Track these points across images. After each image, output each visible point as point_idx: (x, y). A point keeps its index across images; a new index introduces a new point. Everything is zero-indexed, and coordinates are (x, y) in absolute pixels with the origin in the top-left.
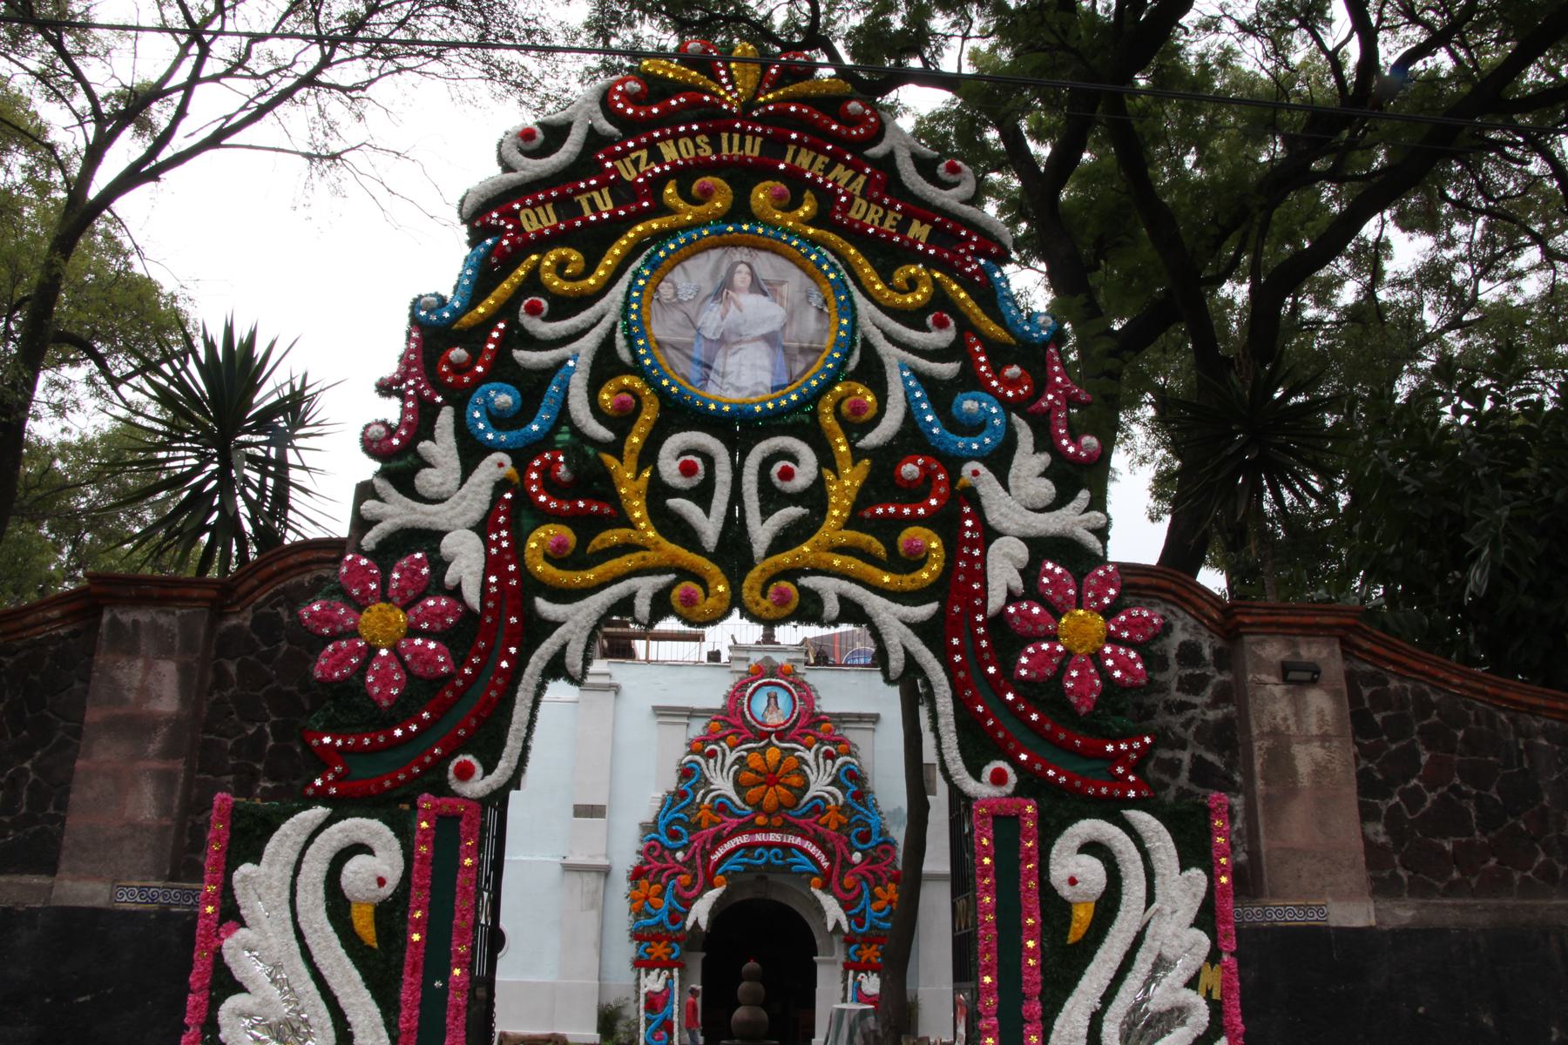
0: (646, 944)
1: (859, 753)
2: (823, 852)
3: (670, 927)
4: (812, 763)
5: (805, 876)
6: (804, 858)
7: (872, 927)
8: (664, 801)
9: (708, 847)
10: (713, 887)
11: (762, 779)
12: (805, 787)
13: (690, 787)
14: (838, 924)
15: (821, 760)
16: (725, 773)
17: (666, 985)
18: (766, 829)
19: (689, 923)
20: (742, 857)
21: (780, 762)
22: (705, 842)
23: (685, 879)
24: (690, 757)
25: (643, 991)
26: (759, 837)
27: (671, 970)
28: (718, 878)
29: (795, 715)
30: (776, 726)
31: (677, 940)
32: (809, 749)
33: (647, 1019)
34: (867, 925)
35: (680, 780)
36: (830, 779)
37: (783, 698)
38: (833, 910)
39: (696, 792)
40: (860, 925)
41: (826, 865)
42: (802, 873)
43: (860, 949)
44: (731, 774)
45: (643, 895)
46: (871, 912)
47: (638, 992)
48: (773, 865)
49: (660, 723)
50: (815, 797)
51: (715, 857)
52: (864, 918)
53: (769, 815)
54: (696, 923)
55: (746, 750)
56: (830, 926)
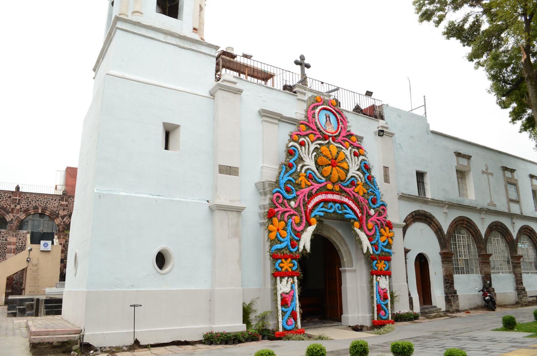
0: (279, 261)
1: (367, 156)
2: (358, 208)
3: (292, 249)
4: (349, 157)
5: (352, 221)
6: (350, 211)
7: (382, 251)
8: (281, 168)
9: (306, 199)
10: (310, 224)
11: (330, 162)
12: (347, 171)
13: (294, 161)
14: (368, 248)
15: (353, 156)
16: (310, 156)
17: (292, 288)
18: (332, 192)
19: (301, 248)
20: (322, 207)
21: (337, 153)
22: (304, 196)
23: (297, 219)
24: (292, 143)
25: (279, 293)
26: (330, 196)
27: (292, 277)
28: (313, 220)
29: (340, 129)
30: (332, 133)
31: (295, 259)
32: (347, 149)
33: (282, 311)
35: (287, 157)
37: (332, 118)
38: (366, 243)
39: (297, 165)
40: (377, 250)
41: (360, 215)
42: (350, 219)
43: (377, 263)
44: (313, 157)
45: (276, 229)
46: (381, 243)
47: (276, 294)
48: (337, 213)
50: (352, 177)
51: (310, 206)
52: (378, 246)
53: (333, 184)
54: (304, 247)
55: (320, 144)
56: (365, 251)
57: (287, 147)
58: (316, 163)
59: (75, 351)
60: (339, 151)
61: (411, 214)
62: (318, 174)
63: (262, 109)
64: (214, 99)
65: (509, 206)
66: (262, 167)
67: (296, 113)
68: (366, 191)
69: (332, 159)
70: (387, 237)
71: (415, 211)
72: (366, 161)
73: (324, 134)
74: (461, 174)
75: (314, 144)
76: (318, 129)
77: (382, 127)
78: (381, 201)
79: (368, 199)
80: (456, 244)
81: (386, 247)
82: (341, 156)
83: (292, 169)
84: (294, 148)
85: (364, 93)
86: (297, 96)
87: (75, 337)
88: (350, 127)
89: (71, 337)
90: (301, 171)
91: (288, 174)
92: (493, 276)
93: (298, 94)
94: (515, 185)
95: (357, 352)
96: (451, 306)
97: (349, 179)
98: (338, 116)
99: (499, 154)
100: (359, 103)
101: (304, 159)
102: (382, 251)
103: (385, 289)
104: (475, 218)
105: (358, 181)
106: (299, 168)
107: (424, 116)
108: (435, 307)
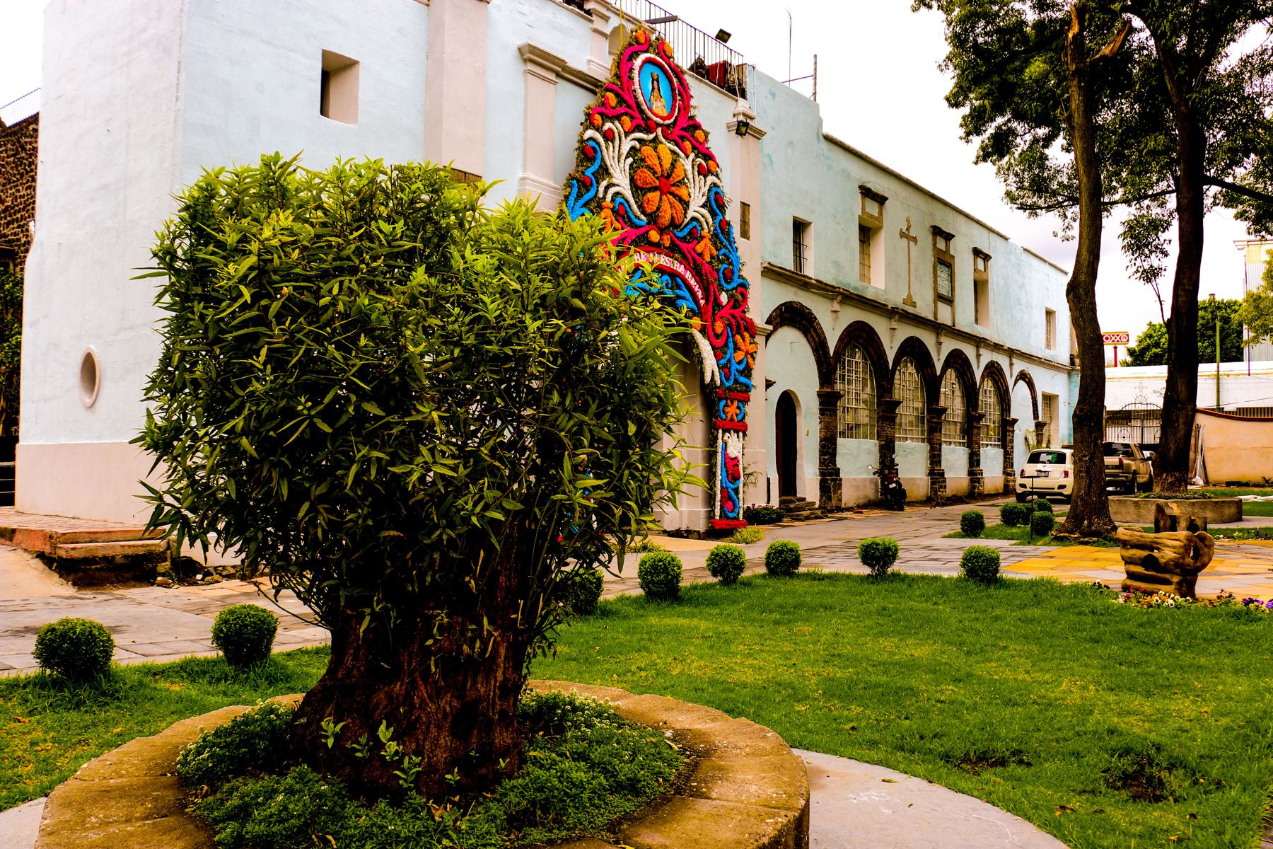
1: (720, 176)
6: (685, 293)
7: (736, 381)
11: (657, 183)
12: (686, 204)
13: (593, 174)
15: (696, 173)
21: (672, 164)
24: (590, 133)
30: (663, 118)
34: (732, 378)
36: (705, 198)
39: (598, 183)
40: (727, 380)
41: (702, 302)
43: (727, 405)
44: (627, 168)
46: (734, 367)
49: (532, 73)
50: (694, 219)
52: (729, 369)
53: (662, 231)
55: (640, 140)
57: (581, 141)
58: (632, 180)
59: (163, 575)
60: (675, 161)
61: (779, 308)
62: (635, 207)
63: (530, 45)
64: (428, 5)
65: (936, 307)
66: (523, 179)
67: (589, 61)
68: (715, 253)
69: (662, 175)
70: (747, 353)
71: (784, 304)
72: (719, 187)
73: (649, 118)
74: (867, 233)
75: (629, 138)
76: (638, 105)
77: (744, 115)
78: (740, 277)
79: (718, 271)
80: (844, 376)
81: (741, 373)
82: (679, 173)
83: (588, 191)
84: (593, 144)
85: (714, 35)
86: (591, 21)
87: (158, 545)
88: (695, 108)
89: (153, 545)
90: (604, 198)
91: (582, 201)
92: (897, 443)
93: (594, 18)
94: (948, 267)
95: (785, 560)
96: (830, 499)
97: (688, 224)
98: (675, 80)
99: (930, 200)
100: (702, 55)
101: (611, 171)
102: (736, 381)
103: (736, 458)
104: (880, 326)
105: (703, 229)
106: (601, 189)
107: (812, 98)
108: (804, 499)
